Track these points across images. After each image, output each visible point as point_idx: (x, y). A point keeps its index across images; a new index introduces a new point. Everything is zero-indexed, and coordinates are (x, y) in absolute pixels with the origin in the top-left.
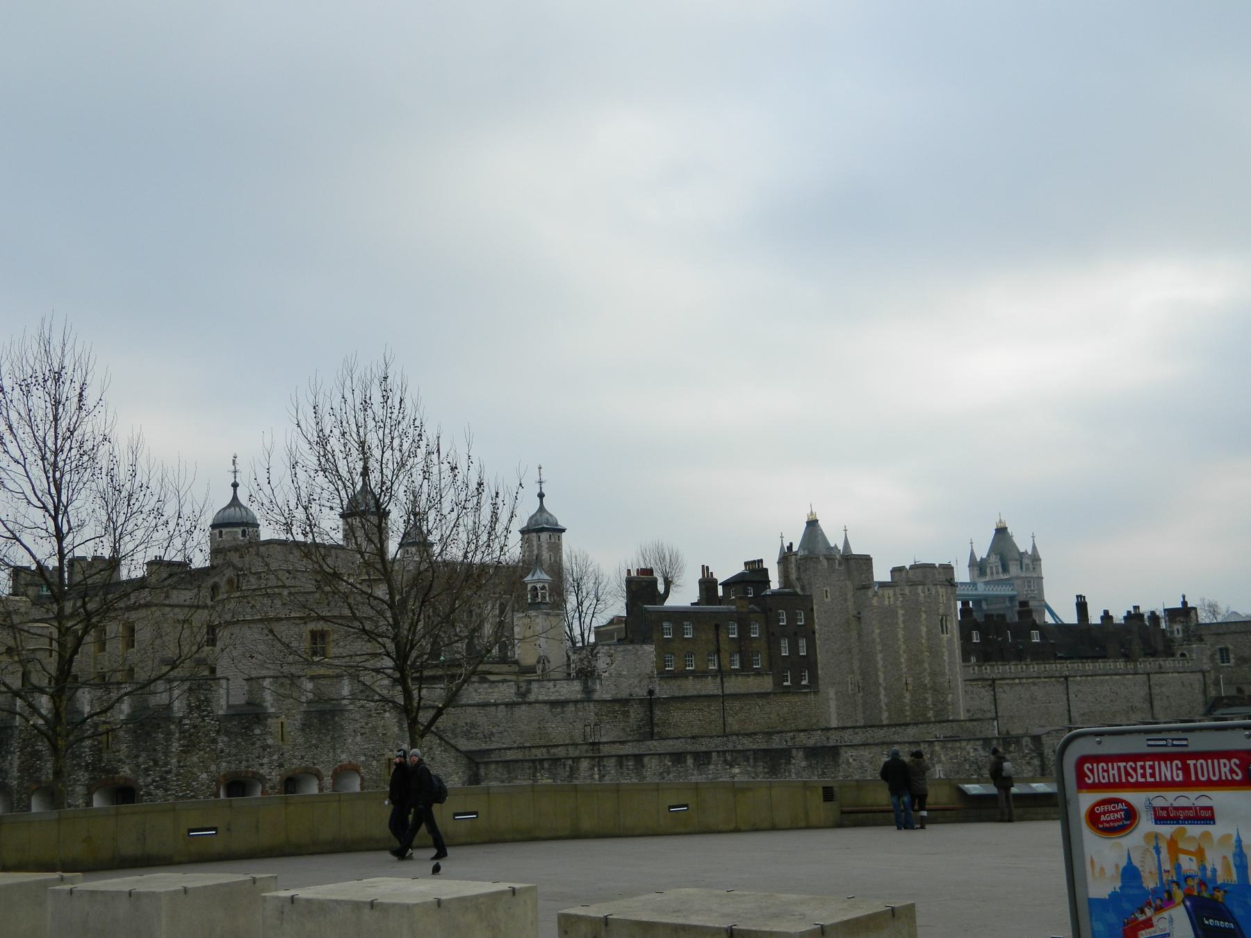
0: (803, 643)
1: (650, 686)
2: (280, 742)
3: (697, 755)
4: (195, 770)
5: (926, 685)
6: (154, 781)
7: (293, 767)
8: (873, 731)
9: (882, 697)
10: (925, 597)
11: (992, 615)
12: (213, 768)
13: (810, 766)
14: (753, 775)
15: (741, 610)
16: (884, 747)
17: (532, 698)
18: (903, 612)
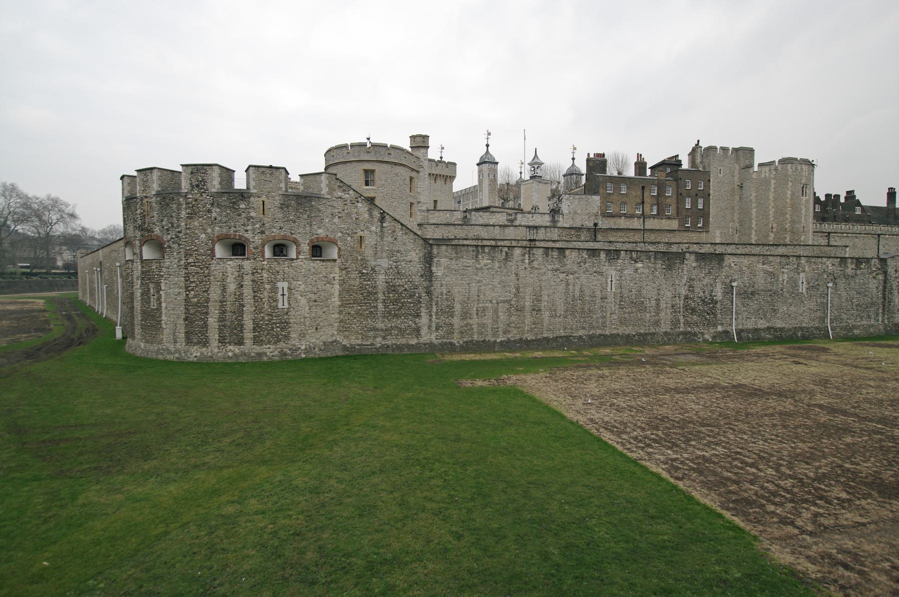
0: (701, 201)
1: (596, 221)
2: (261, 216)
3: (608, 252)
4: (197, 231)
5: (786, 229)
6: (172, 238)
7: (273, 234)
8: (751, 248)
9: (753, 236)
10: (793, 172)
11: (831, 195)
12: (209, 230)
13: (699, 266)
14: (653, 269)
15: (660, 178)
16: (761, 257)
17: (517, 223)
18: (774, 182)
